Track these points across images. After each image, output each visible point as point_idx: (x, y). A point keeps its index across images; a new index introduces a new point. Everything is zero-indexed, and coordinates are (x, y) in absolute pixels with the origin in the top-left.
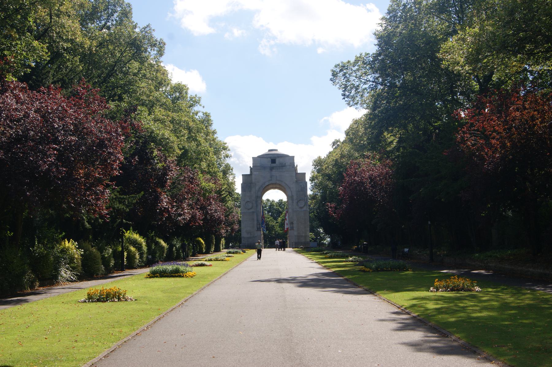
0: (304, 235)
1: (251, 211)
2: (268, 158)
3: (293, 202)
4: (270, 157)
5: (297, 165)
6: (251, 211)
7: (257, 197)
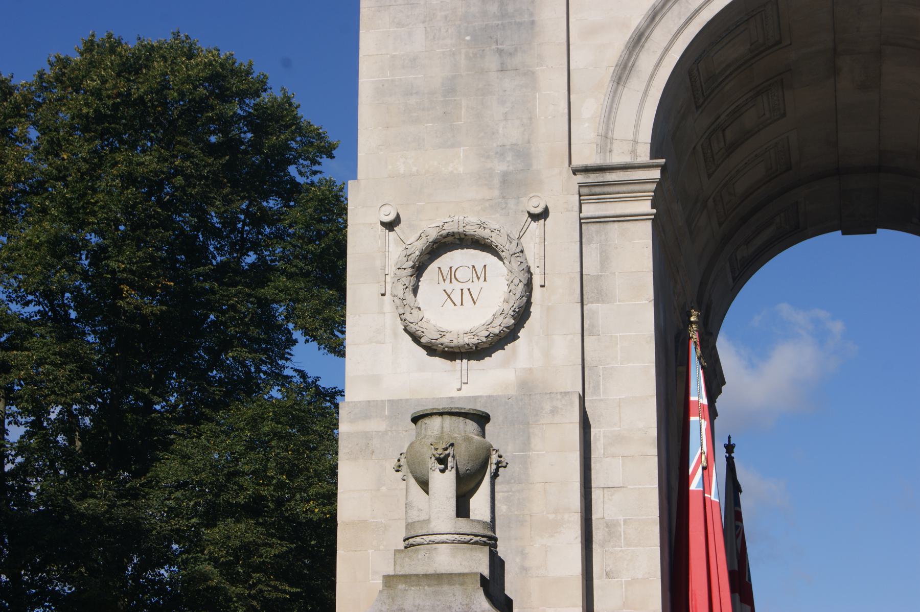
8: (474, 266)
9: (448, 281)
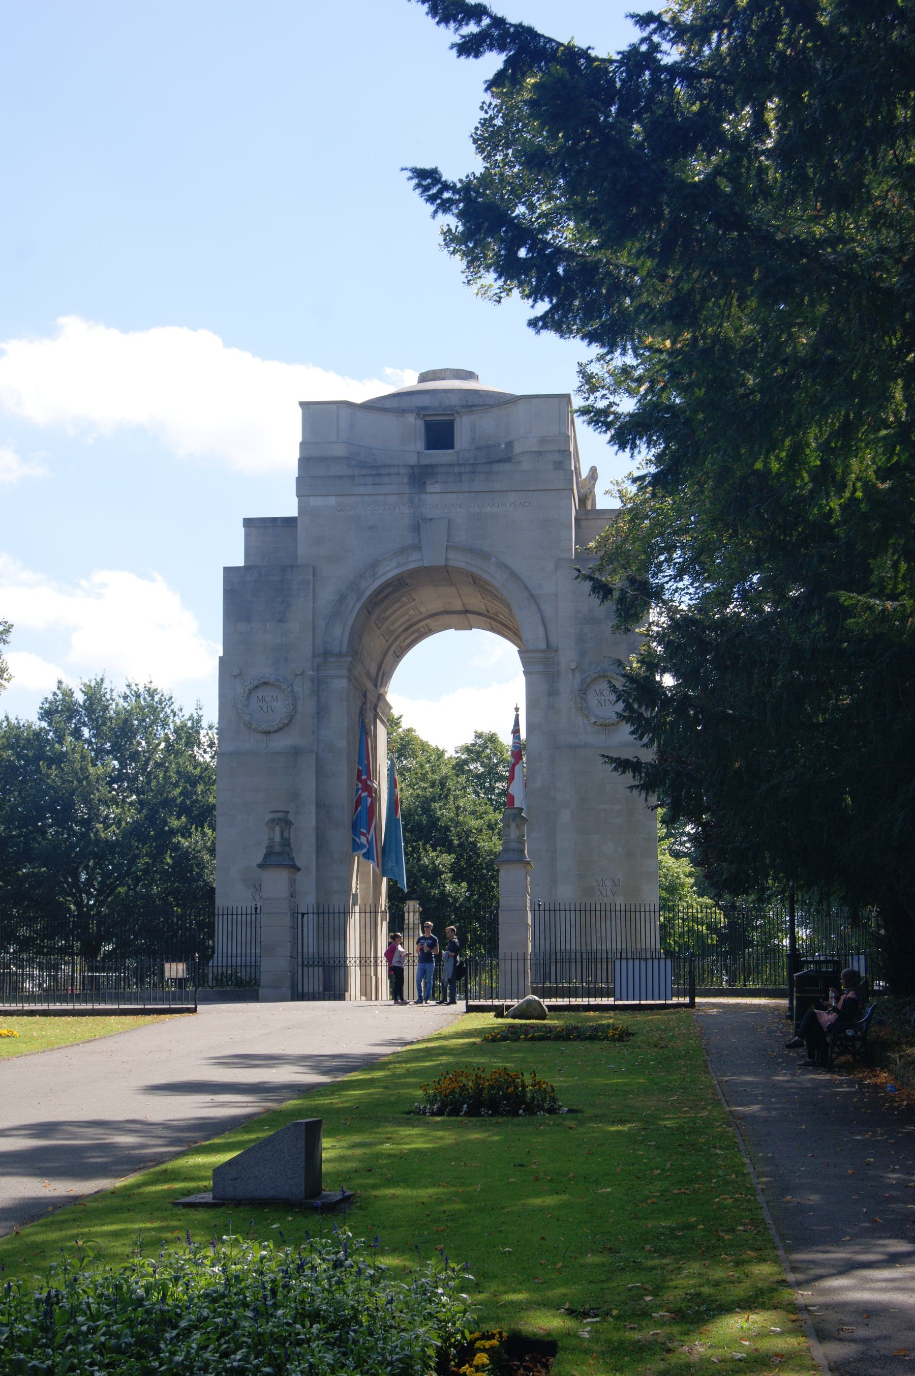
0: (620, 901)
1: (282, 742)
2: (403, 412)
4: (420, 411)
5: (593, 471)
6: (282, 742)
7: (326, 654)
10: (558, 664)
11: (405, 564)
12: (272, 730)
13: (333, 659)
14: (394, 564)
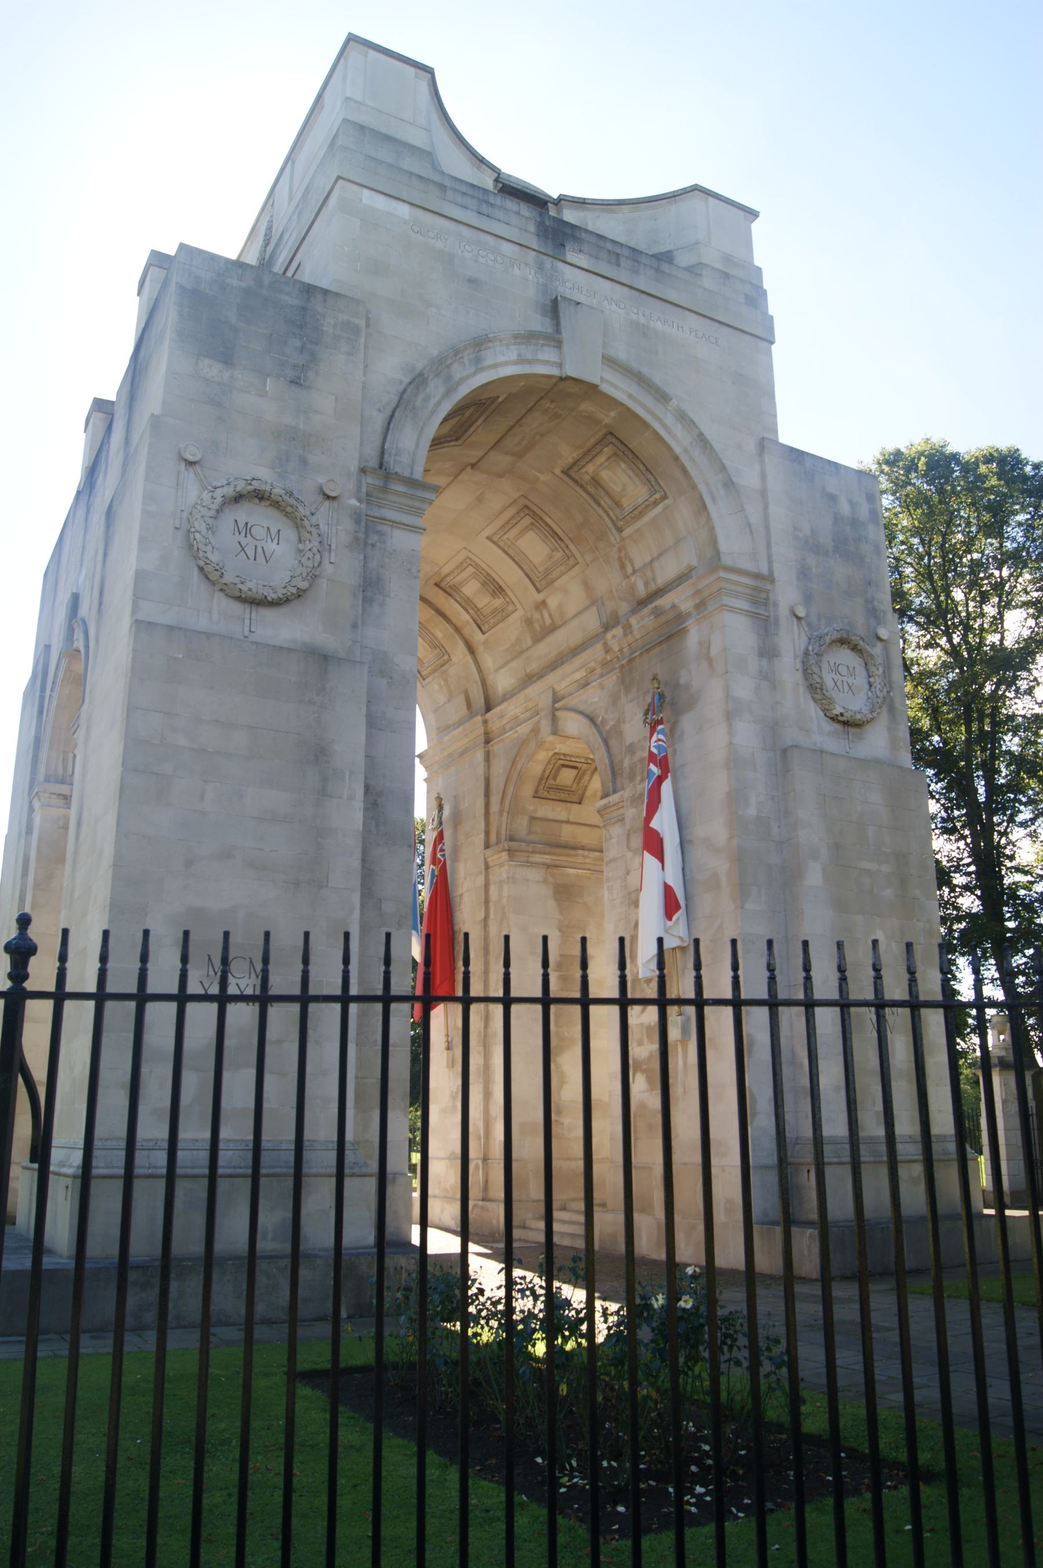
3: (768, 652)
8: (268, 528)
9: (243, 534)
10: (775, 605)
11: (530, 362)
12: (272, 596)
13: (400, 488)
14: (512, 355)
